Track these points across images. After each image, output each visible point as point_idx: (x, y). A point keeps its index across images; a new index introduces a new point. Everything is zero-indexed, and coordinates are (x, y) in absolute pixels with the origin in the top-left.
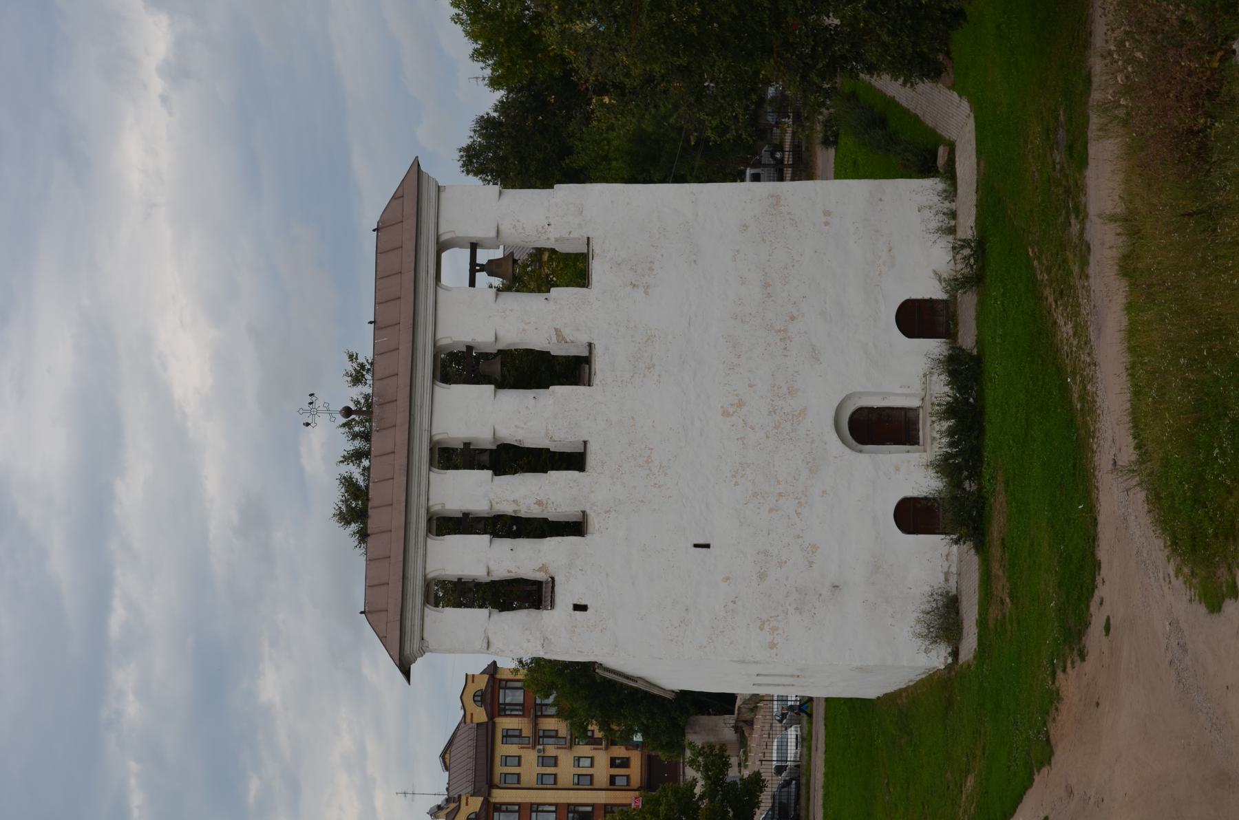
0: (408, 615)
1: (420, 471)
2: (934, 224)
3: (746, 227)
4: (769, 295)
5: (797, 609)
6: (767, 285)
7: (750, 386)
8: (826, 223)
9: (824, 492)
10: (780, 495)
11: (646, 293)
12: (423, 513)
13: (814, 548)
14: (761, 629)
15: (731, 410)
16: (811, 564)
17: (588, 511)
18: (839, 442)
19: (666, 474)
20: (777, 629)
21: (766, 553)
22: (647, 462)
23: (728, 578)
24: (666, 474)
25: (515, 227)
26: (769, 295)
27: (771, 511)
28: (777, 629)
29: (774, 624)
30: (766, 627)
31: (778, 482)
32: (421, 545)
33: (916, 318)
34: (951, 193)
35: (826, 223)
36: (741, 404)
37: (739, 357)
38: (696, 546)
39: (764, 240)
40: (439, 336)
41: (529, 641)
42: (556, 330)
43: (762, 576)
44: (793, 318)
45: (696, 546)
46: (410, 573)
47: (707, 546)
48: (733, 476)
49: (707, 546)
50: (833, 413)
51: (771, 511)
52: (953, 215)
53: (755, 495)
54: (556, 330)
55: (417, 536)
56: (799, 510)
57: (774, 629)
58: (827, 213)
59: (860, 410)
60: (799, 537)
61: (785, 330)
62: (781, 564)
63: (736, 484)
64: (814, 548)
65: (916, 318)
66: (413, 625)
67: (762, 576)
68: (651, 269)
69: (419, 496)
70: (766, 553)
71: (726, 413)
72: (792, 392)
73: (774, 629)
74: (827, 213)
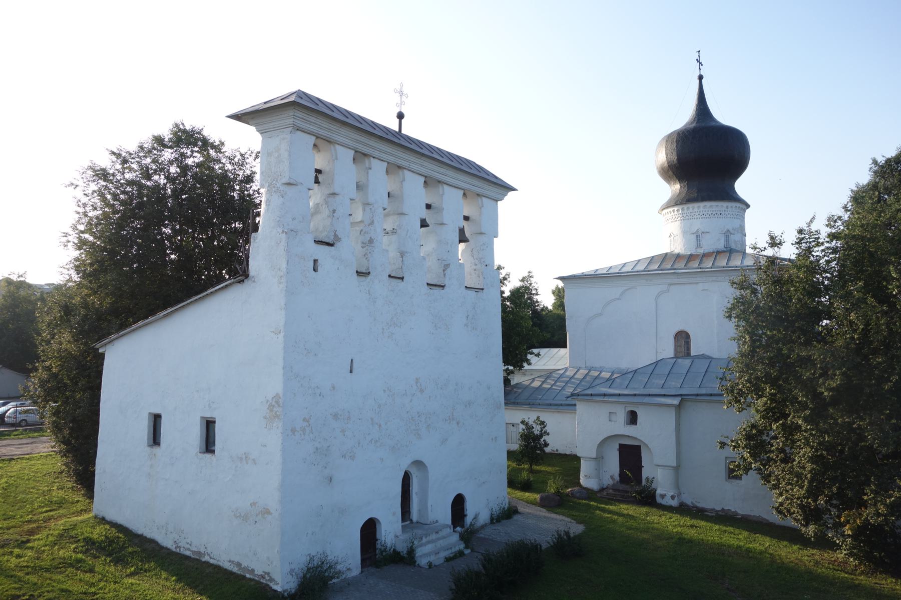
0: (320, 121)
1: (393, 155)
5: (317, 449)
10: (380, 426)
13: (353, 458)
14: (304, 420)
16: (344, 456)
17: (370, 277)
21: (349, 418)
23: (334, 388)
30: (305, 424)
32: (350, 143)
36: (422, 391)
40: (446, 187)
41: (294, 219)
44: (458, 423)
46: (344, 131)
49: (351, 372)
51: (372, 419)
57: (304, 430)
64: (353, 458)
67: (336, 416)
71: (417, 380)
73: (304, 430)
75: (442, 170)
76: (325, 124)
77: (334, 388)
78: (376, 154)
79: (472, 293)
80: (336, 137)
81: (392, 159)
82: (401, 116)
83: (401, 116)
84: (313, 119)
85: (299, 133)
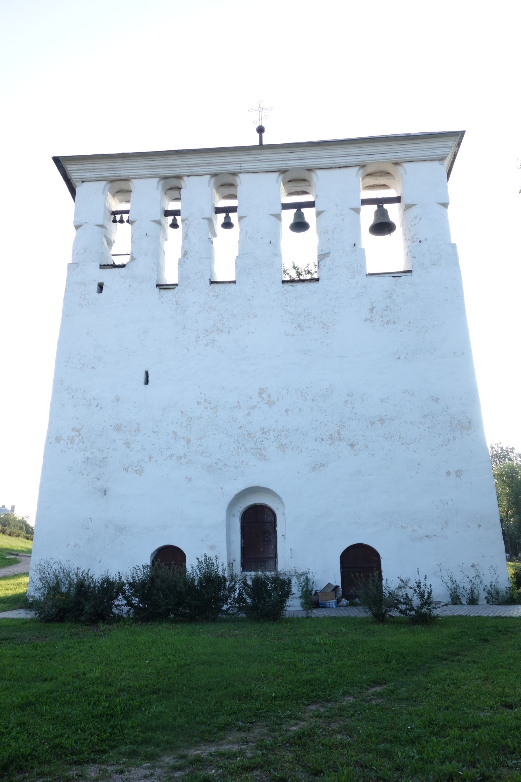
1: (208, 164)
2: (458, 578)
3: (437, 400)
4: (372, 423)
5: (88, 459)
6: (382, 421)
7: (287, 411)
8: (448, 473)
9: (190, 479)
10: (189, 441)
11: (366, 320)
12: (176, 172)
13: (140, 472)
14: (73, 429)
15: (265, 396)
16: (126, 469)
18: (236, 491)
19: (207, 345)
20: (72, 443)
21: (138, 430)
22: (218, 330)
23: (118, 400)
24: (207, 345)
25: (415, 218)
26: (372, 423)
27: (175, 433)
28: (72, 443)
29: (77, 440)
30: (74, 433)
31: (200, 439)
33: (360, 562)
34: (496, 598)
35: (448, 473)
36: (270, 403)
37: (313, 400)
38: (147, 374)
39: (425, 416)
40: (318, 172)
42: (329, 253)
43: (118, 428)
44: (352, 445)
45: (147, 374)
46: (129, 163)
47: (147, 382)
48: (206, 400)
49: (147, 382)
50: (263, 485)
51: (175, 433)
52: (473, 601)
53: (189, 419)
54: (329, 253)
55: (157, 167)
56: (174, 458)
58: (459, 473)
59: (274, 515)
60: (151, 458)
61: (340, 439)
62: (128, 444)
63: (199, 403)
64: (140, 472)
65: (360, 562)
66: (90, 170)
67: (118, 428)
68: (388, 322)
69: (188, 166)
70: (138, 430)
71: (261, 391)
72: (283, 447)
73: (72, 440)
74: (459, 473)
75: (301, 154)
76: (105, 165)
77: (118, 400)
78: (185, 171)
79: (390, 279)
80: (125, 173)
81: (212, 169)
82: (261, 130)
83: (261, 130)
84: (90, 166)
85: (84, 183)
